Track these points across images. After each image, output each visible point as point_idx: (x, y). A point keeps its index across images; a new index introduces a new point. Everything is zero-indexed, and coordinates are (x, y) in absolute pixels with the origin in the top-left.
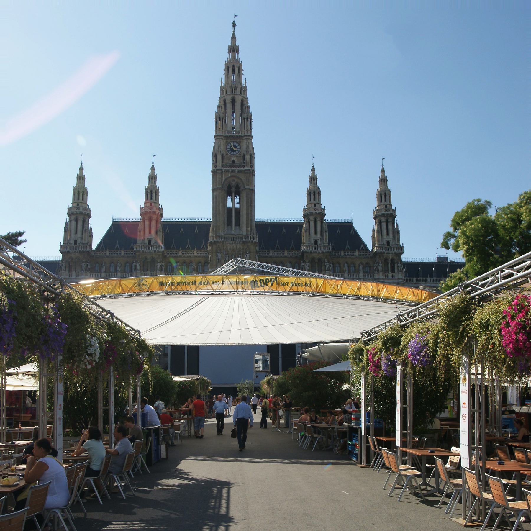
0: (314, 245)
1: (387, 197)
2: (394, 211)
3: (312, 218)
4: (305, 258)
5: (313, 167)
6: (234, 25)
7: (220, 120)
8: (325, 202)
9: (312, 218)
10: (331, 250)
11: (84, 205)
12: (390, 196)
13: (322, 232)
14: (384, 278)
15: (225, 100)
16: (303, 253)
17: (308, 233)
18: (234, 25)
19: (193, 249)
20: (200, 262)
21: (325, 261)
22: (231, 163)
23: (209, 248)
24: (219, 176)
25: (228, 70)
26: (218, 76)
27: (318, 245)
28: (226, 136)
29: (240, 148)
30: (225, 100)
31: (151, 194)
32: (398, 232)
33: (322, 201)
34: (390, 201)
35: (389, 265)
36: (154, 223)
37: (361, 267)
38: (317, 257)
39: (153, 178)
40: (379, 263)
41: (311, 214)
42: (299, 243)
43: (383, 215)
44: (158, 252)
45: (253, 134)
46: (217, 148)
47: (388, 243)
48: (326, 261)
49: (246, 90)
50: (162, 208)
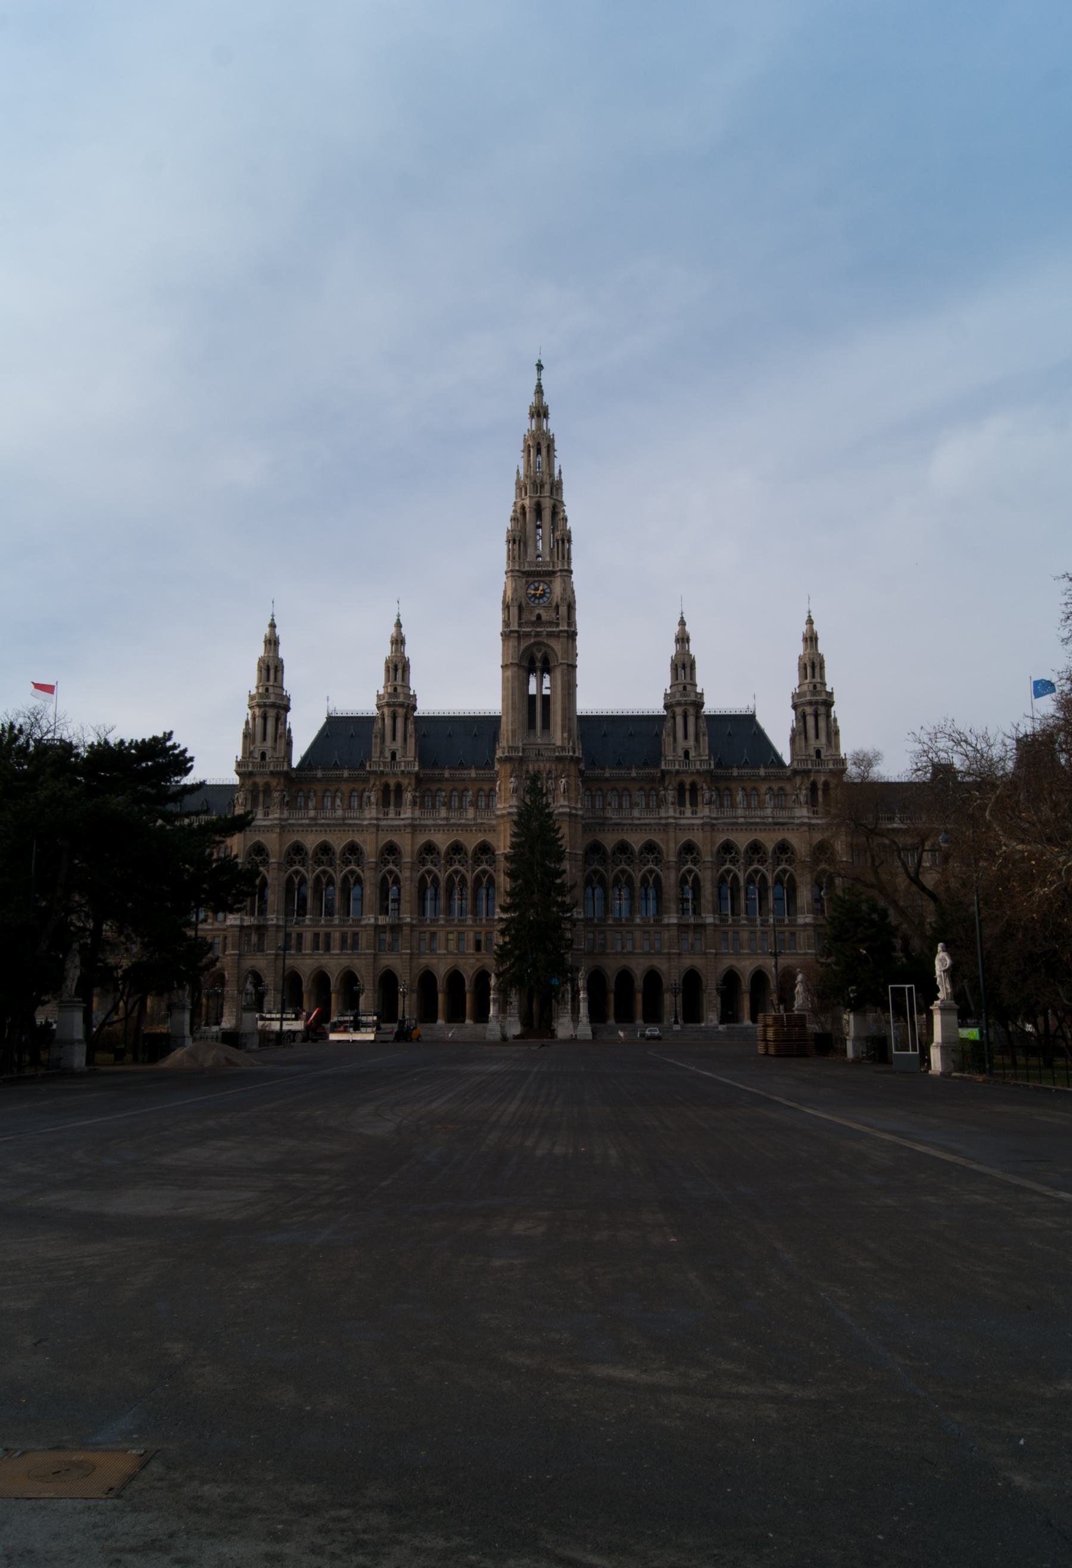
0: (682, 759)
1: (817, 670)
2: (831, 694)
3: (679, 710)
4: (667, 782)
5: (682, 618)
6: (540, 367)
7: (514, 542)
8: (703, 681)
9: (679, 710)
10: (712, 767)
11: (278, 691)
12: (822, 668)
14: (811, 815)
15: (523, 507)
16: (664, 773)
17: (671, 739)
19: (468, 768)
20: (481, 789)
21: (702, 788)
22: (534, 619)
23: (497, 767)
24: (513, 643)
25: (529, 451)
27: (691, 758)
28: (524, 573)
29: (550, 593)
30: (523, 507)
31: (396, 669)
32: (837, 733)
33: (699, 680)
34: (822, 676)
35: (820, 793)
38: (688, 781)
39: (398, 642)
40: (800, 789)
41: (679, 704)
42: (655, 757)
43: (810, 703)
44: (409, 773)
45: (573, 567)
46: (509, 593)
47: (818, 753)
48: (705, 787)
49: (561, 489)
50: (415, 696)
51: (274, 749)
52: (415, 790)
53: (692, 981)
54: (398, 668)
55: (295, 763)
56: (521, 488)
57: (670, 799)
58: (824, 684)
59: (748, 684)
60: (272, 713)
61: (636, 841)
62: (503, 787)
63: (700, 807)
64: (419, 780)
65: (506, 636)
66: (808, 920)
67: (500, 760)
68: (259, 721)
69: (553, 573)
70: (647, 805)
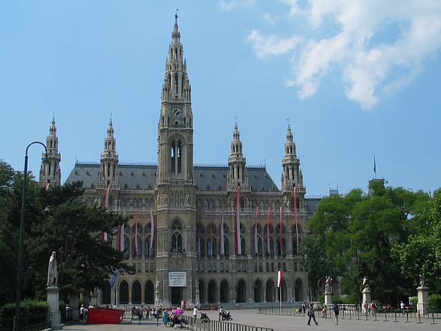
2: (298, 160)
3: (235, 166)
6: (176, 17)
8: (246, 153)
9: (235, 166)
12: (295, 149)
13: (243, 176)
18: (176, 17)
22: (174, 123)
26: (164, 56)
29: (182, 112)
30: (170, 75)
36: (111, 168)
37: (273, 204)
41: (235, 163)
43: (290, 164)
46: (164, 112)
51: (54, 179)
52: (118, 198)
53: (241, 285)
54: (111, 143)
55: (62, 184)
56: (169, 67)
57: (232, 204)
58: (295, 156)
59: (266, 156)
60: (53, 162)
61: (217, 223)
62: (161, 198)
63: (245, 208)
64: (120, 194)
65: (162, 131)
66: (290, 258)
67: (159, 186)
68: (47, 166)
69: (183, 104)
70: (221, 207)
